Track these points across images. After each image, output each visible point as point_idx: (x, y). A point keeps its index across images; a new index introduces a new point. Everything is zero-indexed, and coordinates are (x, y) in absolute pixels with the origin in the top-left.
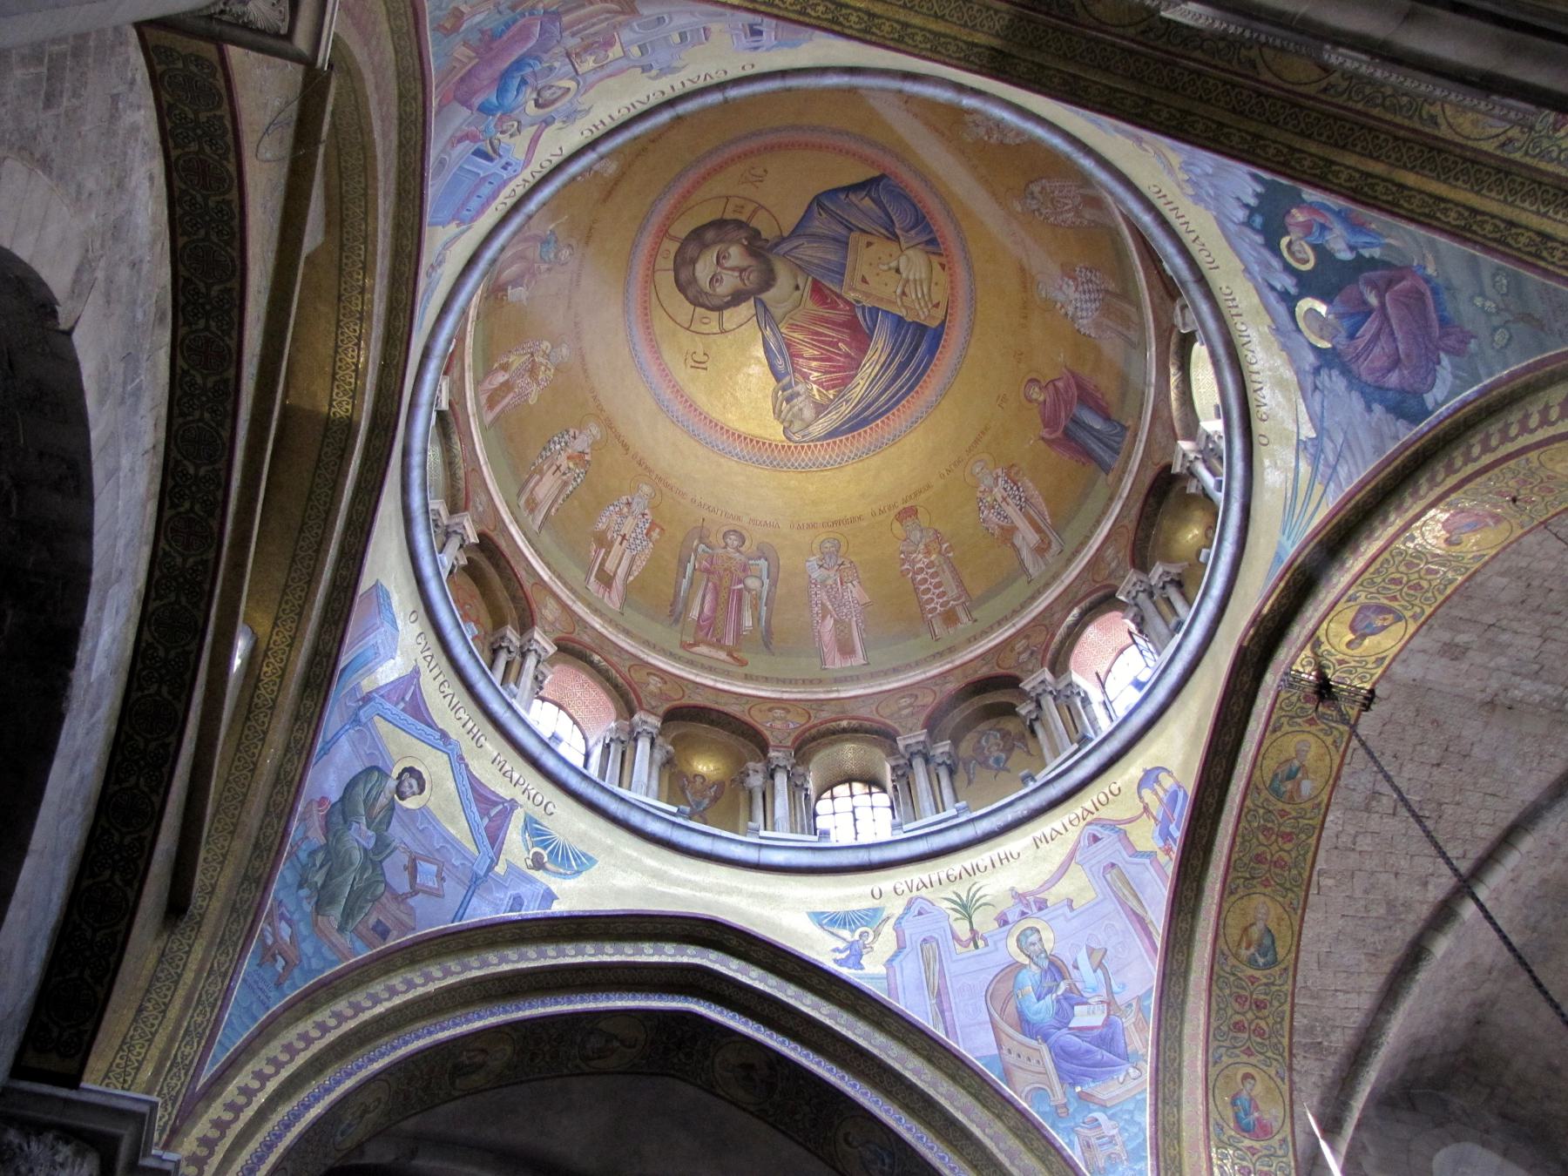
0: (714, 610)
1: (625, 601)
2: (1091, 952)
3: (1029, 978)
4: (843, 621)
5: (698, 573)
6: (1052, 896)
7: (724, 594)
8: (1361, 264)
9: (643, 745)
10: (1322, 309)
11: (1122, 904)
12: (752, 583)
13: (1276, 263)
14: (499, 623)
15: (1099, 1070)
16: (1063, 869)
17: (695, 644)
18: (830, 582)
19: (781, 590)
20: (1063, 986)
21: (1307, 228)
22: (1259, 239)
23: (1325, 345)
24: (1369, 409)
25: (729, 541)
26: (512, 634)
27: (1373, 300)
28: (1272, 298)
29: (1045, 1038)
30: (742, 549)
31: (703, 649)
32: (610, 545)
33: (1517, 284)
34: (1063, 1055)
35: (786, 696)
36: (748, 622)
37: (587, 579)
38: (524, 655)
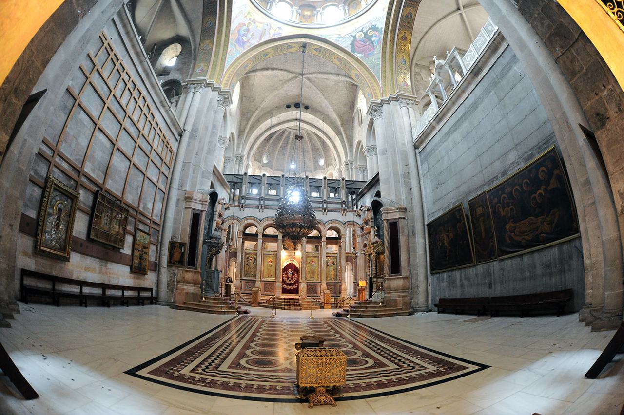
2: (253, 34)
3: (244, 28)
6: (257, 24)
8: (372, 42)
10: (363, 36)
11: (262, 33)
13: (367, 29)
15: (240, 45)
16: (261, 23)
20: (246, 33)
21: (375, 34)
22: (370, 27)
23: (357, 37)
24: (350, 44)
27: (367, 44)
28: (361, 28)
29: (239, 35)
33: (379, 64)
34: (238, 38)
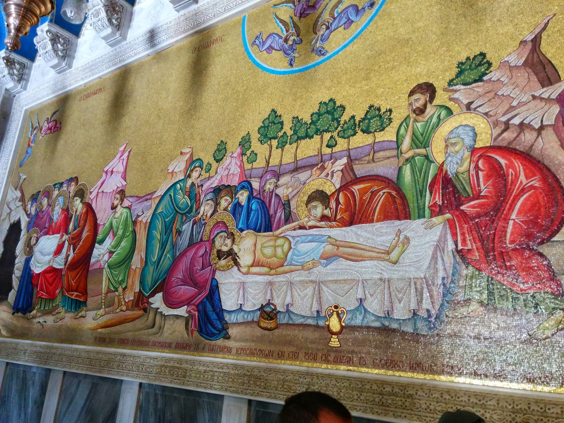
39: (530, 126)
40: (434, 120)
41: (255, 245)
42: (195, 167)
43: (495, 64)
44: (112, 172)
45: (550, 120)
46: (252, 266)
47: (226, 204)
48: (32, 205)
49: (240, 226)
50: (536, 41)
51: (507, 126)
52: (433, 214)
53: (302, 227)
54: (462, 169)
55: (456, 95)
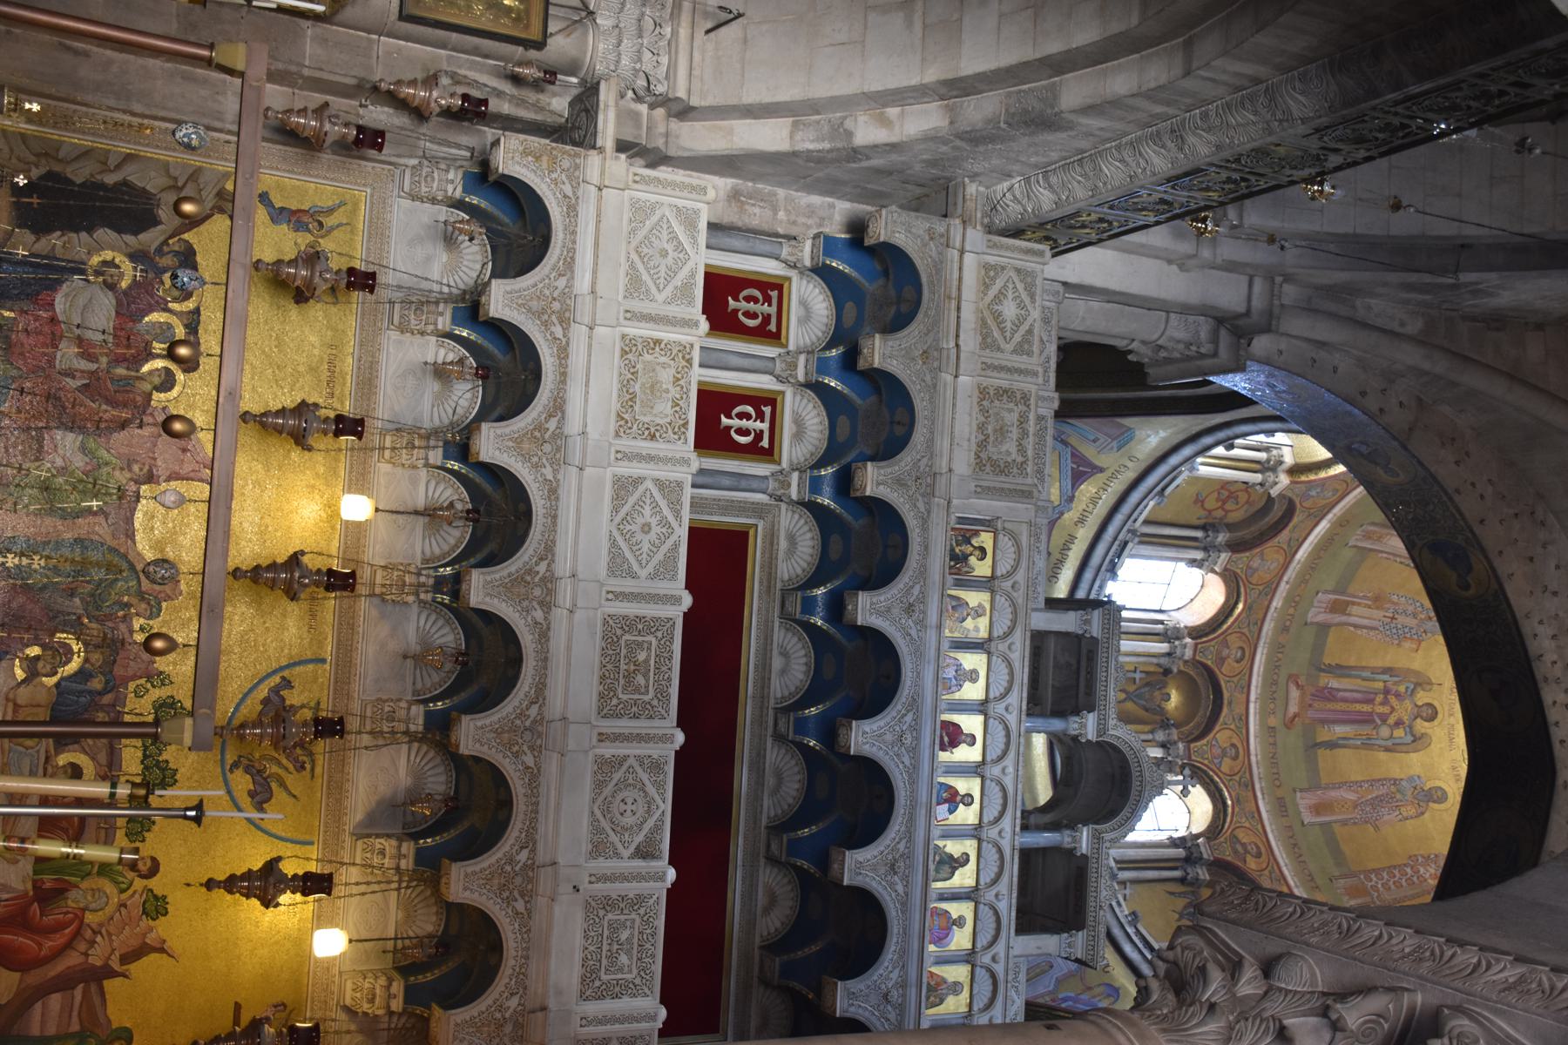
0: (1345, 700)
1: (1324, 628)
4: (1355, 807)
5: (1381, 685)
7: (1366, 708)
9: (1163, 647)
12: (1385, 731)
14: (1230, 527)
17: (1298, 685)
18: (1399, 796)
19: (1383, 756)
25: (1425, 708)
26: (1222, 538)
30: (1419, 721)
31: (1295, 693)
32: (1377, 608)
35: (1253, 758)
36: (1340, 730)
37: (1326, 592)
38: (1205, 549)
39: (92, 947)
40: (121, 879)
41: (39, 706)
42: (152, 607)
43: (151, 923)
44: (184, 450)
45: (91, 960)
46: (15, 704)
47: (93, 661)
48: (177, 253)
49: (63, 683)
50: (162, 950)
51: (95, 932)
52: (35, 882)
53: (47, 759)
54: (70, 903)
55: (137, 896)
